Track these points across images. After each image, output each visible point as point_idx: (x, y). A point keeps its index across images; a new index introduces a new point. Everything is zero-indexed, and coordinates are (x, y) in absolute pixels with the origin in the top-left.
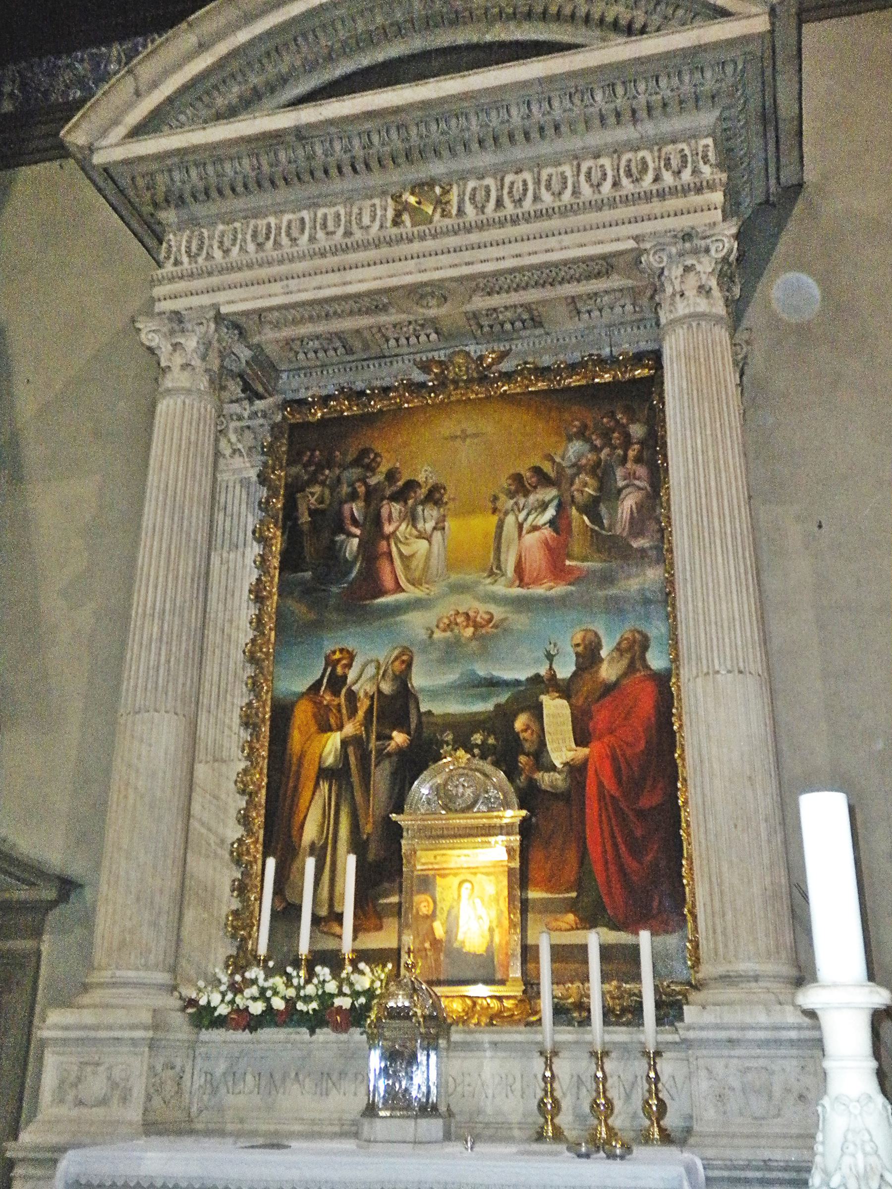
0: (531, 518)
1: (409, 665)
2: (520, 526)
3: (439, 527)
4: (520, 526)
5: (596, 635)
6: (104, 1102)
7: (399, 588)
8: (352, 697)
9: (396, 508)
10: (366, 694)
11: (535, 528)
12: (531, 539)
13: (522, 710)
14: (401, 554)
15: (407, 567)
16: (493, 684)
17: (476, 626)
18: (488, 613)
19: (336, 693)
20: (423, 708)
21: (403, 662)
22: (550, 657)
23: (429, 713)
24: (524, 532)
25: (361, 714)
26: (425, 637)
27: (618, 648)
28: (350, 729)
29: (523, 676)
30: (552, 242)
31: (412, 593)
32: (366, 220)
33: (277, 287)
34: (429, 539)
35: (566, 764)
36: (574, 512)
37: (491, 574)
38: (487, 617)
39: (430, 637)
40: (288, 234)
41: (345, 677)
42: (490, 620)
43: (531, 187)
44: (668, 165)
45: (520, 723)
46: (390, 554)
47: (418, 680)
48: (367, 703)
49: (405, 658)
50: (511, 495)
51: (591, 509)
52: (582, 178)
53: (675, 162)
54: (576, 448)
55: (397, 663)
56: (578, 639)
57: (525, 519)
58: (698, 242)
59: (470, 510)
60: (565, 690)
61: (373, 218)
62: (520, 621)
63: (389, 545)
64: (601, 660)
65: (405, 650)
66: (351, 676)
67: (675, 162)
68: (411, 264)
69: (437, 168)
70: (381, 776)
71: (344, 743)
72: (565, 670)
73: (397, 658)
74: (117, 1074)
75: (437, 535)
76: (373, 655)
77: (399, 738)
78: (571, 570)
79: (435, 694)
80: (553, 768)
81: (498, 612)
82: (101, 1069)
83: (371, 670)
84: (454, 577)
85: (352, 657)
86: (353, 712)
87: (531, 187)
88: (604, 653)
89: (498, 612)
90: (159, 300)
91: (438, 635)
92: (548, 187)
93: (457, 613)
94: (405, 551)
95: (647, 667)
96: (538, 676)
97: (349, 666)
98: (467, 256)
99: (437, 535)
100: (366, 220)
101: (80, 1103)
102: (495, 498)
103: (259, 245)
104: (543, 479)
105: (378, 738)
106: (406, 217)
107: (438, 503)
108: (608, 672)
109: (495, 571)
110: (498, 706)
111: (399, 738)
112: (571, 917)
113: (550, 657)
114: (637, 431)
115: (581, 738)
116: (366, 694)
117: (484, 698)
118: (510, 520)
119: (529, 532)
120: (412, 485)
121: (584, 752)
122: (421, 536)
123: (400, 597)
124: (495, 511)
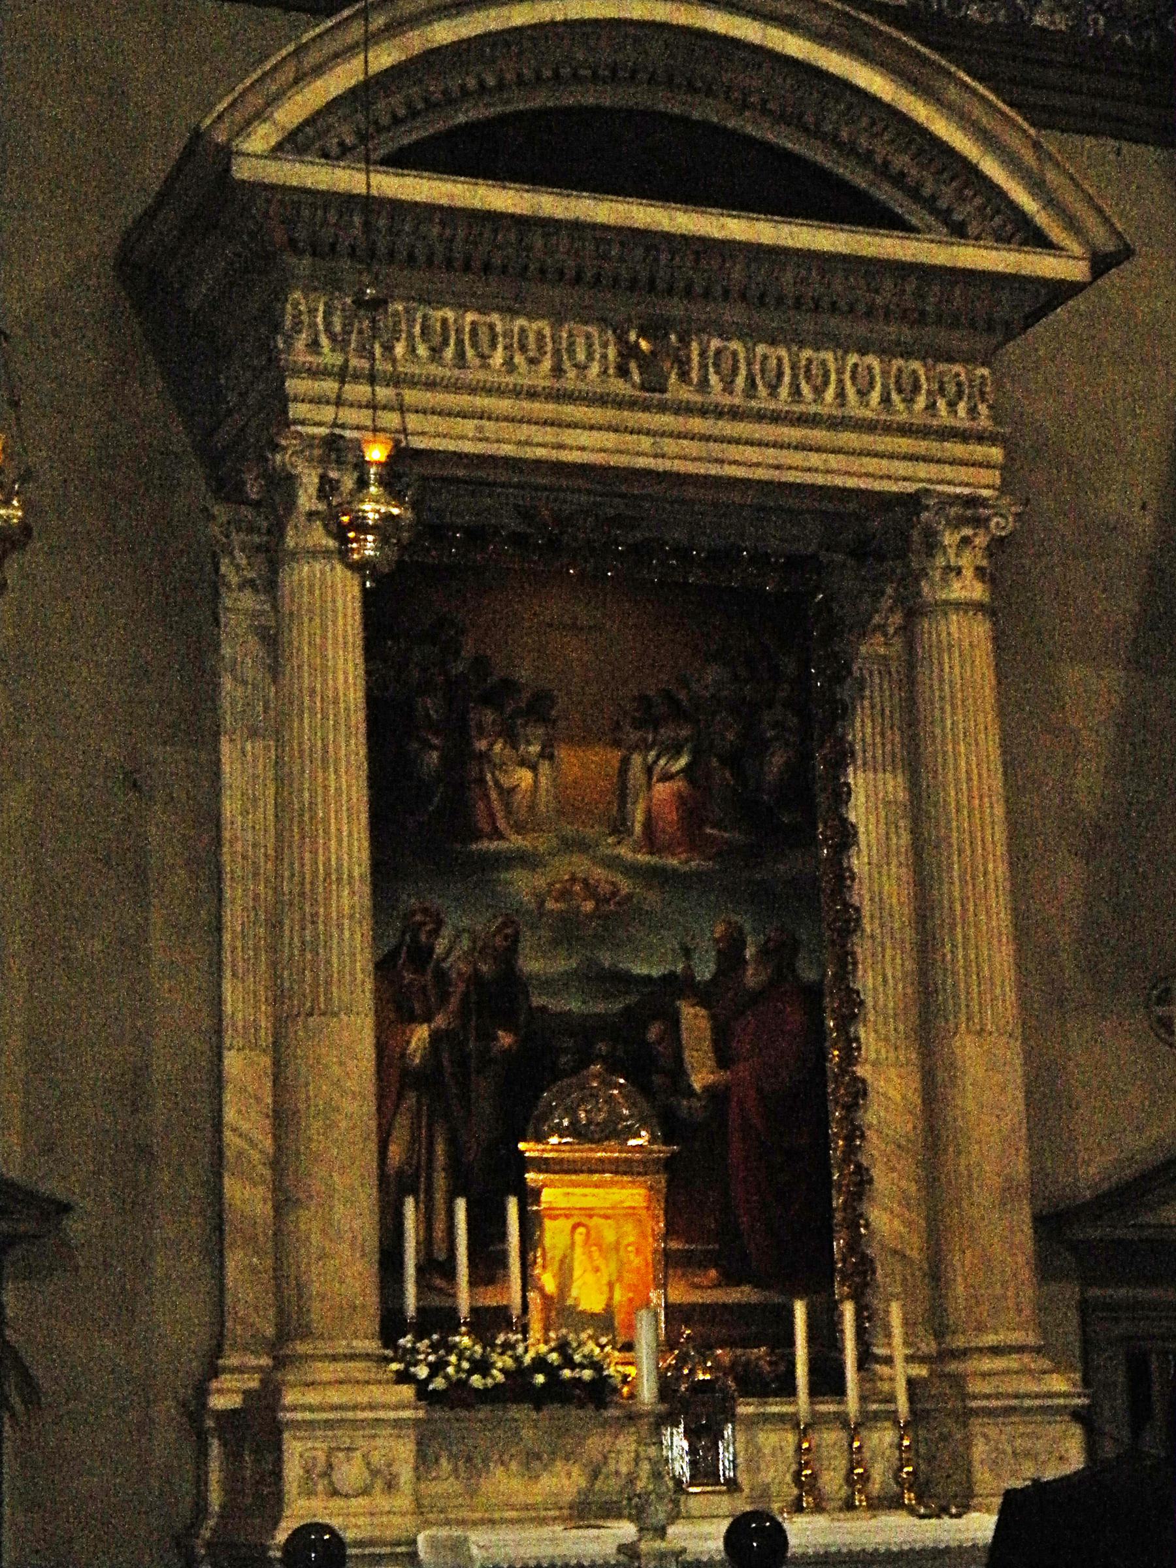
0: (662, 762)
1: (515, 939)
2: (649, 770)
3: (547, 754)
4: (649, 770)
5: (740, 930)
6: (365, 1491)
7: (498, 835)
8: (441, 976)
9: (489, 716)
10: (460, 974)
11: (667, 777)
12: (662, 790)
13: (655, 1018)
14: (497, 782)
15: (507, 806)
16: (624, 980)
17: (600, 901)
18: (613, 883)
19: (420, 969)
20: (537, 1001)
21: (506, 937)
22: (687, 952)
23: (543, 1009)
24: (655, 779)
25: (454, 1002)
26: (533, 906)
27: (764, 952)
28: (440, 1021)
29: (655, 973)
30: (815, 459)
31: (517, 841)
32: (581, 356)
33: (469, 426)
34: (534, 768)
35: (706, 1089)
36: (715, 762)
37: (614, 831)
38: (609, 888)
39: (542, 904)
40: (475, 345)
41: (431, 950)
42: (614, 894)
43: (787, 371)
44: (942, 390)
45: (654, 1032)
46: (482, 781)
47: (531, 964)
48: (462, 987)
49: (509, 931)
50: (638, 725)
51: (732, 760)
52: (847, 376)
53: (952, 389)
54: (712, 674)
55: (498, 939)
56: (719, 930)
57: (655, 762)
58: (982, 511)
59: (584, 739)
60: (704, 995)
61: (590, 357)
62: (652, 898)
63: (481, 771)
64: (746, 962)
65: (508, 922)
66: (440, 947)
67: (952, 389)
68: (646, 443)
69: (676, 308)
70: (483, 1086)
71: (436, 1038)
72: (705, 972)
73: (499, 930)
74: (376, 1459)
75: (545, 767)
76: (466, 922)
77: (506, 1039)
78: (712, 840)
79: (547, 984)
80: (691, 1093)
81: (625, 886)
82: (358, 1454)
83: (465, 943)
84: (569, 830)
85: (440, 923)
86: (444, 998)
87: (787, 371)
88: (749, 953)
89: (625, 886)
90: (295, 400)
91: (550, 905)
92: (808, 379)
93: (573, 879)
94: (506, 782)
95: (797, 978)
96: (672, 974)
97: (435, 933)
98: (715, 449)
99: (545, 767)
100: (581, 356)
101: (335, 1493)
102: (617, 727)
103: (433, 349)
104: (678, 713)
105: (478, 1039)
106: (633, 366)
107: (544, 719)
108: (752, 977)
109: (619, 827)
110: (627, 1008)
111: (506, 1039)
112: (713, 1273)
113: (687, 952)
114: (790, 666)
115: (723, 1060)
116: (460, 974)
117: (607, 996)
118: (637, 759)
119: (658, 781)
120: (509, 686)
121: (724, 1076)
122: (523, 763)
123: (494, 845)
124: (617, 743)
